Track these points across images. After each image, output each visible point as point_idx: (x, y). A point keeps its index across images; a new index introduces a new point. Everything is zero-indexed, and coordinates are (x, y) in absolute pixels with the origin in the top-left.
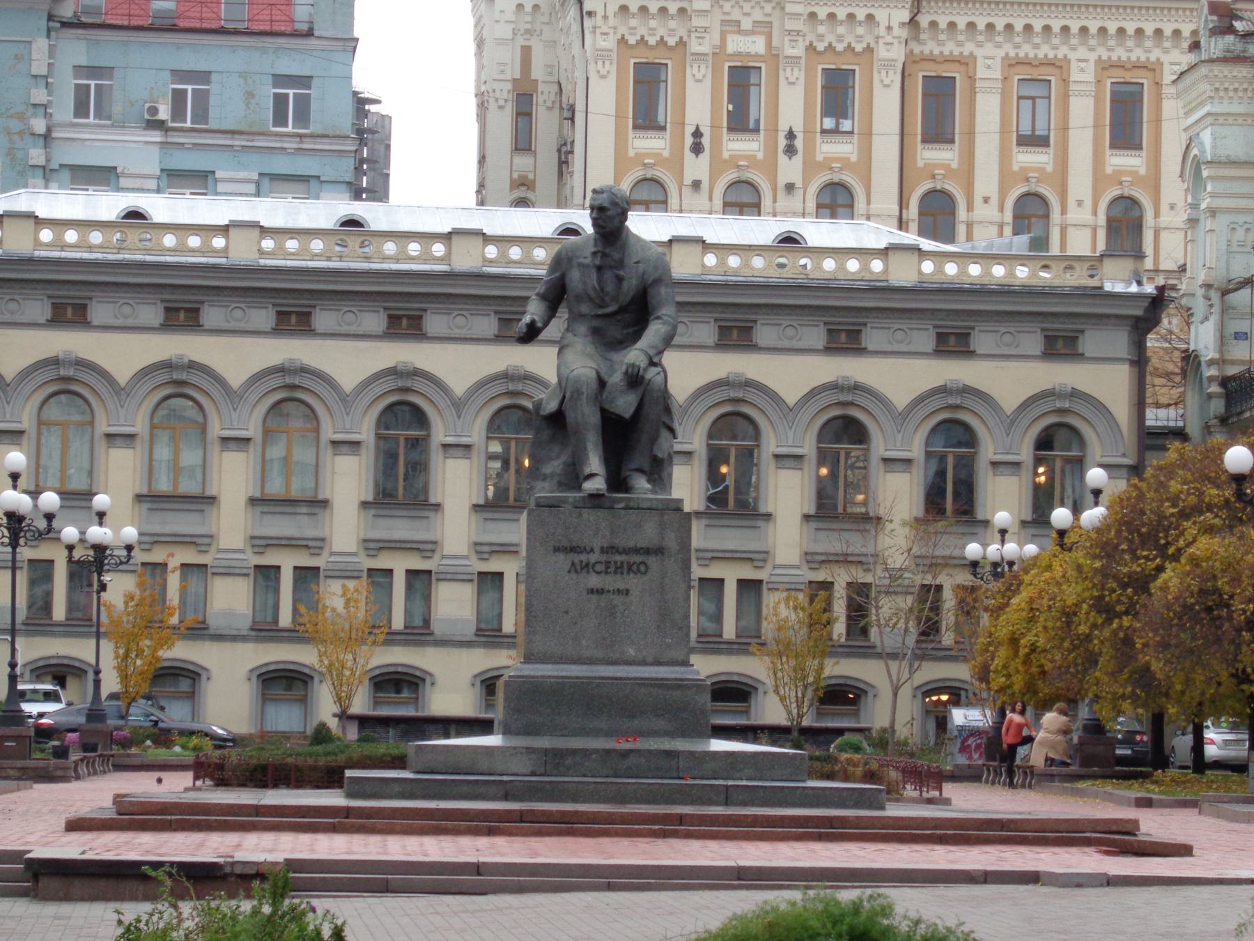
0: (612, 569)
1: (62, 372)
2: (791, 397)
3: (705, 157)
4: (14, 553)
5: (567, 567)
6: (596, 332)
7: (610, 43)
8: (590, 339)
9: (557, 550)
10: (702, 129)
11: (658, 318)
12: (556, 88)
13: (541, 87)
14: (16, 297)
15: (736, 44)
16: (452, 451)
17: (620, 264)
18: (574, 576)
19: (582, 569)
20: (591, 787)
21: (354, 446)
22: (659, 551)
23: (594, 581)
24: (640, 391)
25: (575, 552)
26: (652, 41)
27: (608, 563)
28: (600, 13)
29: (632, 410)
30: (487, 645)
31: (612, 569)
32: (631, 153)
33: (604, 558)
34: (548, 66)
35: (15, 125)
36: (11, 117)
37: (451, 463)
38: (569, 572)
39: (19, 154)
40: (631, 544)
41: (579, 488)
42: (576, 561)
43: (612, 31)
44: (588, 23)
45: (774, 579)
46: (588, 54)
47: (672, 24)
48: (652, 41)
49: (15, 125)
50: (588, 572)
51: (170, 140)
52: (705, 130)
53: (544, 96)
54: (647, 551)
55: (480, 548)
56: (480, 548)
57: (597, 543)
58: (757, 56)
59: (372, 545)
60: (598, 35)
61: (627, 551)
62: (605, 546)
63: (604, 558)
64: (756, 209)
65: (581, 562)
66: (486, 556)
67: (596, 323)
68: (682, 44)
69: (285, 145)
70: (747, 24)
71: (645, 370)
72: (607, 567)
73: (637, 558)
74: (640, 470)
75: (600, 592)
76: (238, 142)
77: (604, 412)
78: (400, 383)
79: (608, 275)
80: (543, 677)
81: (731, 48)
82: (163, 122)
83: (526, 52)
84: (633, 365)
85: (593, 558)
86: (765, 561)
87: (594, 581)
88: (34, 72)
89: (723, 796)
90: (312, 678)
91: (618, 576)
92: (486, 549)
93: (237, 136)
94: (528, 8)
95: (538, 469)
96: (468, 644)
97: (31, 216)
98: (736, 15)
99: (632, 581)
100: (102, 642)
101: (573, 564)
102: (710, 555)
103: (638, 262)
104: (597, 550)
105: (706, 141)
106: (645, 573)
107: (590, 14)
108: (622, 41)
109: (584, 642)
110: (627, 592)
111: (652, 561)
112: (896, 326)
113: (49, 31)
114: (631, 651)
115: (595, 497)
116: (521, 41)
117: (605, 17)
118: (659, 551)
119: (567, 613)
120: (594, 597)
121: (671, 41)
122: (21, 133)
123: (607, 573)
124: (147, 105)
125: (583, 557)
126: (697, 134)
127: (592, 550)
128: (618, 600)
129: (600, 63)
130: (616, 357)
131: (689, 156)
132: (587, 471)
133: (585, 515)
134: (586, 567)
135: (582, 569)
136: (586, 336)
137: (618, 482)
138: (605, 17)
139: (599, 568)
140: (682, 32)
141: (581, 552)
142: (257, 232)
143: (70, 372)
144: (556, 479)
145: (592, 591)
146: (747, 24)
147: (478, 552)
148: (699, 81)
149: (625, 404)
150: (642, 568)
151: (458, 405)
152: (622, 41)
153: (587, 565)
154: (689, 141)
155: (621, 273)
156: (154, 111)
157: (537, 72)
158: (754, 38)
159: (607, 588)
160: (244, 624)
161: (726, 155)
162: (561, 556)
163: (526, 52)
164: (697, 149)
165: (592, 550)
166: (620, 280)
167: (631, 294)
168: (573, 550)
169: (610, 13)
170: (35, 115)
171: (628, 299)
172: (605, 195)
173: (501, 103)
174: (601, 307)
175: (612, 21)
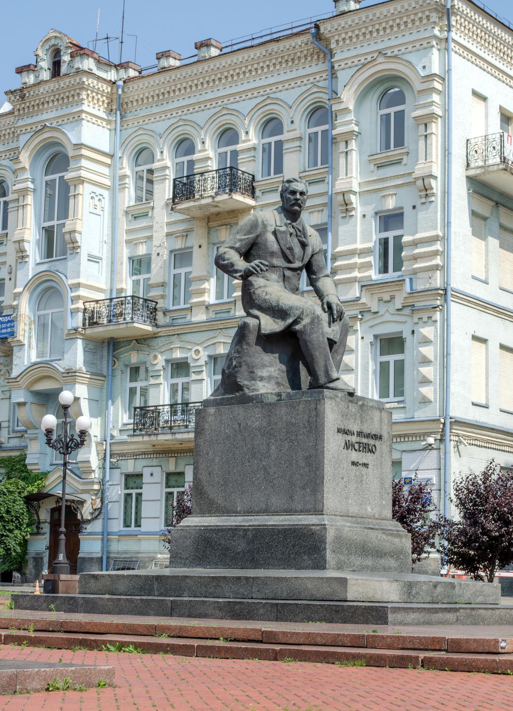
9: (339, 431)
18: (345, 450)
23: (355, 456)
33: (358, 439)
63: (358, 439)
73: (371, 442)
85: (354, 439)
95: (252, 372)
111: (377, 443)
118: (380, 438)
119: (343, 478)
120: (354, 467)
125: (349, 438)
133: (350, 407)
136: (278, 282)
168: (346, 432)
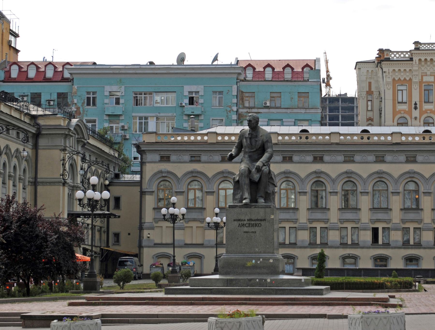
0: (251, 226)
1: (224, 175)
2: (427, 176)
3: (418, 110)
4: (174, 225)
5: (237, 226)
6: (250, 157)
7: (390, 80)
8: (248, 159)
9: (234, 220)
10: (417, 103)
11: (267, 152)
12: (378, 93)
13: (374, 93)
14: (212, 155)
15: (425, 79)
16: (332, 194)
17: (256, 136)
18: (240, 228)
19: (242, 226)
20: (236, 290)
21: (305, 193)
22: (264, 220)
23: (246, 229)
24: (260, 173)
25: (240, 221)
26: (402, 79)
27: (249, 224)
28: (387, 72)
29: (258, 179)
30: (343, 248)
31: (251, 226)
32: (397, 110)
33: (249, 222)
34: (376, 87)
35: (229, 109)
36: (227, 107)
37: (332, 197)
38: (238, 226)
39: (230, 117)
40: (256, 218)
41: (242, 202)
42: (240, 224)
43: (391, 77)
44: (384, 74)
45: (424, 227)
46: (385, 83)
47: (408, 74)
48: (402, 79)
49: (229, 109)
50: (244, 227)
51: (270, 111)
52: (418, 103)
53: (376, 94)
54: (261, 220)
55: (341, 221)
56: (341, 221)
57: (247, 218)
58: (432, 82)
59: (310, 221)
60: (387, 78)
61: (254, 220)
62: (249, 219)
63: (249, 222)
64: (433, 124)
65: (242, 224)
66: (343, 223)
67: (250, 154)
68: (410, 79)
69: (301, 111)
70: (428, 73)
71: (262, 167)
72: (249, 225)
73: (258, 222)
74: (262, 197)
75: (247, 232)
76: (289, 111)
77: (250, 180)
78: (317, 175)
79: (253, 140)
80: (231, 258)
81: (424, 80)
82: (268, 106)
83: (370, 83)
84: (258, 166)
85: (245, 222)
86: (421, 222)
87: (246, 229)
88: (233, 94)
89: (275, 292)
90: (295, 258)
91: (252, 228)
92: (342, 221)
93: (289, 109)
94: (370, 71)
96: (338, 248)
97: (215, 133)
98: (425, 71)
99: (256, 229)
100: (175, 249)
101: (239, 224)
102: (405, 221)
103: (261, 136)
104: (246, 220)
105: (418, 106)
106: (260, 226)
107: (385, 72)
108: (394, 79)
109: (243, 247)
110: (255, 232)
111: (263, 223)
112: (425, 155)
113: (237, 83)
114: (257, 250)
115: (246, 204)
116: (368, 81)
117: (389, 73)
118: (264, 220)
119: (238, 239)
120: (246, 234)
121: (408, 79)
122: (230, 111)
123: (249, 227)
124: (264, 102)
125: (242, 222)
126: (416, 104)
127: (245, 220)
128: (252, 235)
129: (388, 86)
130: (254, 164)
131: (413, 110)
132: (244, 197)
134: (243, 225)
135: (242, 226)
137: (254, 200)
138: (389, 73)
139: (247, 225)
140: (411, 76)
141: (242, 221)
142: (277, 134)
143: (227, 175)
144: (239, 200)
145: (245, 232)
146: (428, 73)
147: (340, 222)
148: (415, 89)
149: (256, 177)
150: (260, 225)
151: (334, 181)
152: (394, 79)
153: (244, 224)
154: (413, 106)
155: (257, 139)
156: (266, 103)
157: (373, 89)
158: (431, 77)
159: (249, 231)
160: (307, 244)
161: (424, 110)
162: (236, 222)
163: (370, 83)
164: (416, 108)
165: (245, 220)
166: (256, 141)
167: (260, 145)
168: (239, 220)
169: (390, 72)
170: (233, 106)
171: (259, 147)
172: (251, 117)
173: (363, 98)
174: (251, 149)
175: (391, 74)
